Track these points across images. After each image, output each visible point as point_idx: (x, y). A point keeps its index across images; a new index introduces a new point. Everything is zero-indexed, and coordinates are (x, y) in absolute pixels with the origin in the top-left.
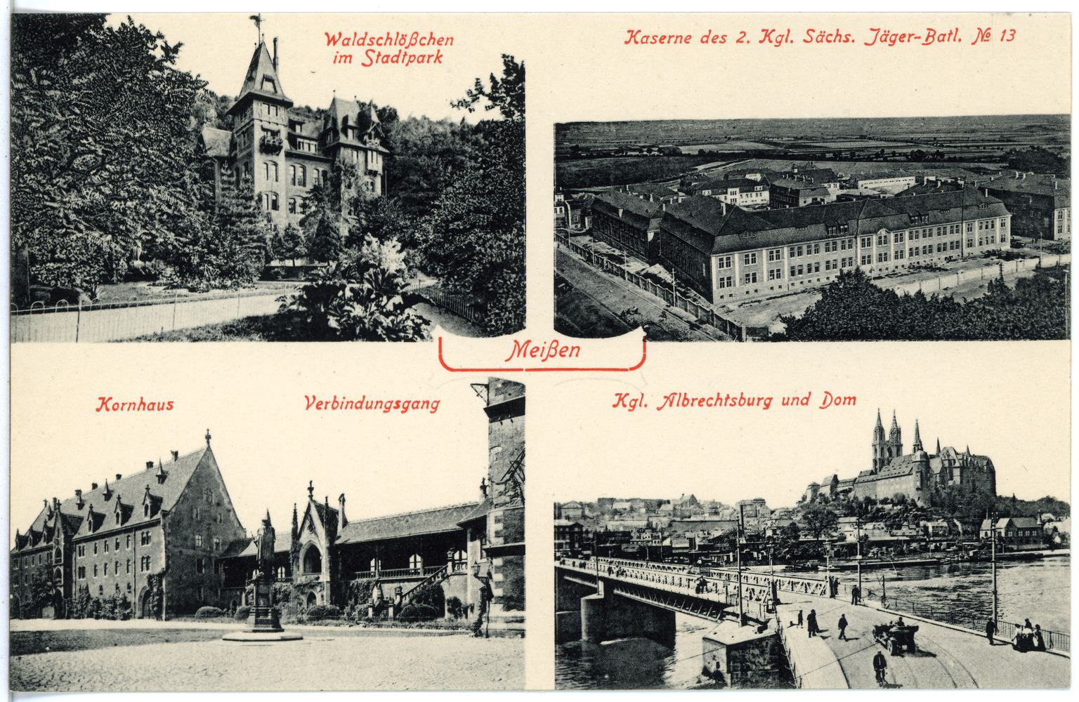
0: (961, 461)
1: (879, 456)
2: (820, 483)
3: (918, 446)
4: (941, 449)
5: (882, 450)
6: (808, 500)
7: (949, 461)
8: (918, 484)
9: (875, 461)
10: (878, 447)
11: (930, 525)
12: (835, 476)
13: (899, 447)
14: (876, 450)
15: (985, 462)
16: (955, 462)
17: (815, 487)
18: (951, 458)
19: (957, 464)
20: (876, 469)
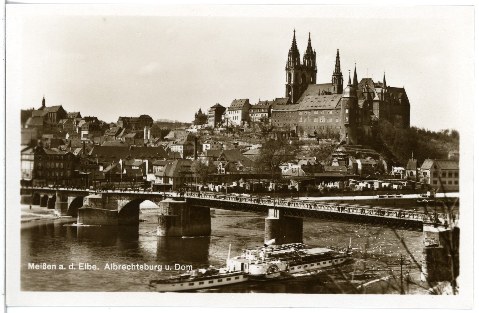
0: (380, 95)
1: (292, 83)
2: (226, 104)
3: (338, 76)
4: (359, 81)
6: (211, 123)
7: (369, 94)
8: (348, 119)
9: (288, 87)
11: (358, 162)
12: (248, 101)
14: (290, 75)
15: (400, 95)
16: (374, 96)
17: (219, 110)
18: (370, 91)
19: (376, 98)
20: (288, 95)
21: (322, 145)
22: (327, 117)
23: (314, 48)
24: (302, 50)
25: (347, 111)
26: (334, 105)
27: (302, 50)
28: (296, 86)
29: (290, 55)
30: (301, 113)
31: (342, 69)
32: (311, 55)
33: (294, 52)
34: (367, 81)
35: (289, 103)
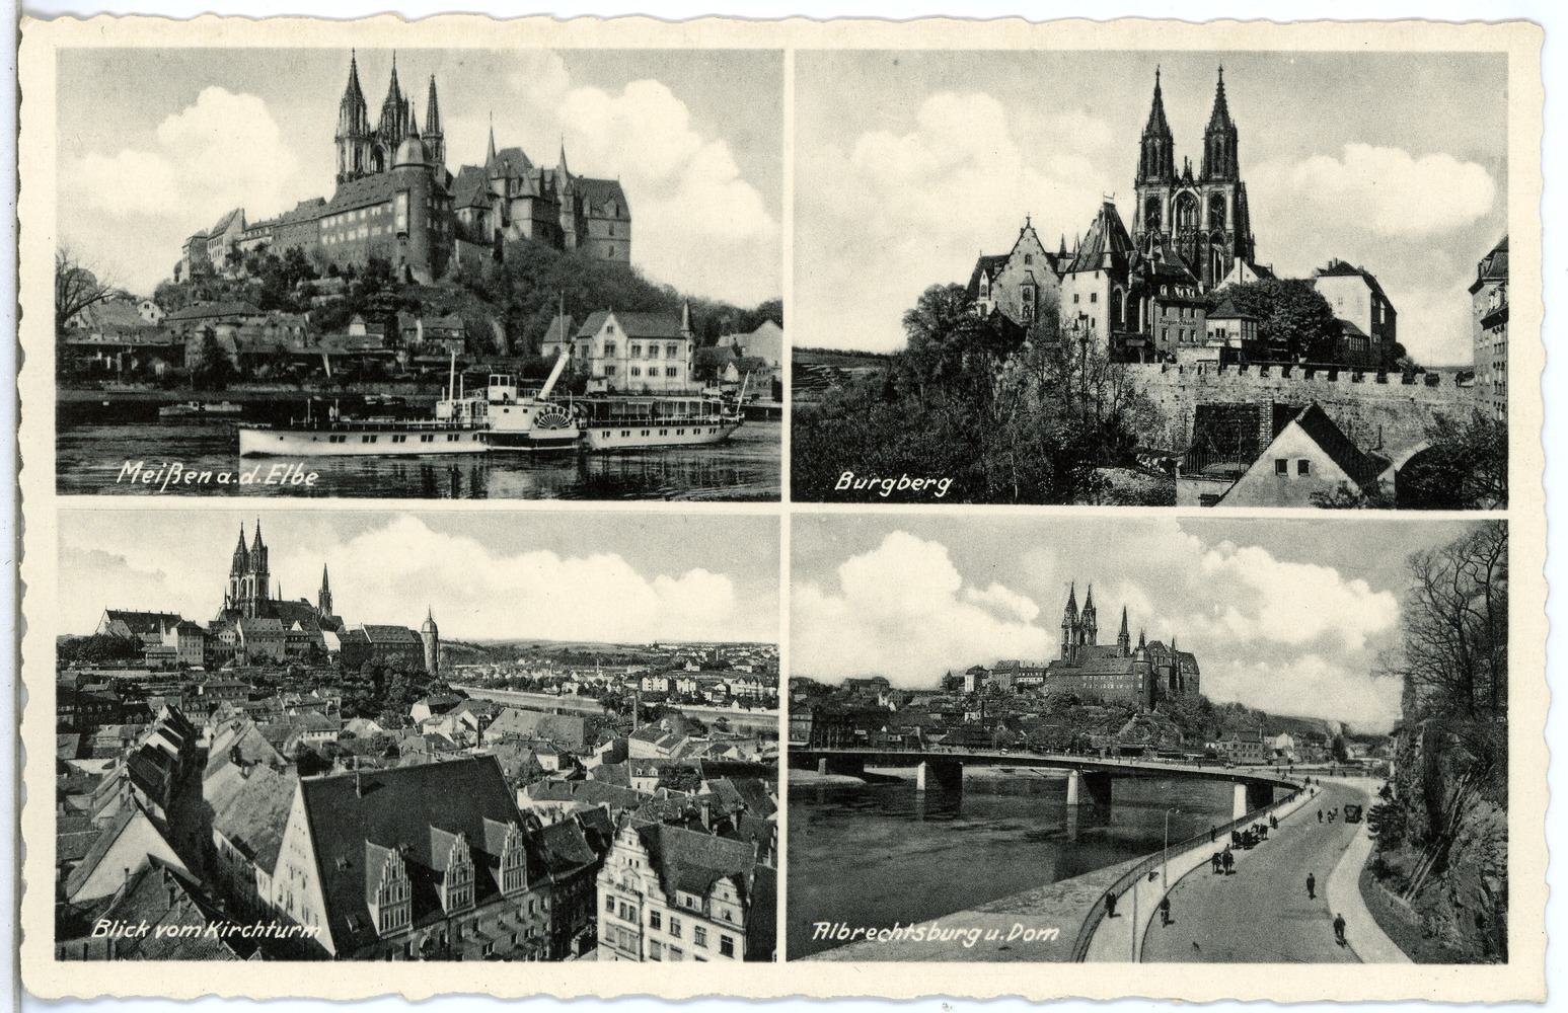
3: (1124, 636)
5: (1074, 632)
6: (969, 685)
8: (1140, 686)
9: (1065, 648)
10: (1070, 630)
13: (1093, 632)
14: (1067, 633)
21: (1110, 715)
22: (1116, 682)
23: (1096, 603)
24: (1081, 607)
25: (1141, 677)
26: (1125, 668)
27: (1081, 607)
28: (1074, 647)
29: (1067, 610)
30: (1085, 678)
31: (1130, 628)
32: (1090, 610)
33: (1072, 605)
34: (1158, 644)
35: (1069, 666)
